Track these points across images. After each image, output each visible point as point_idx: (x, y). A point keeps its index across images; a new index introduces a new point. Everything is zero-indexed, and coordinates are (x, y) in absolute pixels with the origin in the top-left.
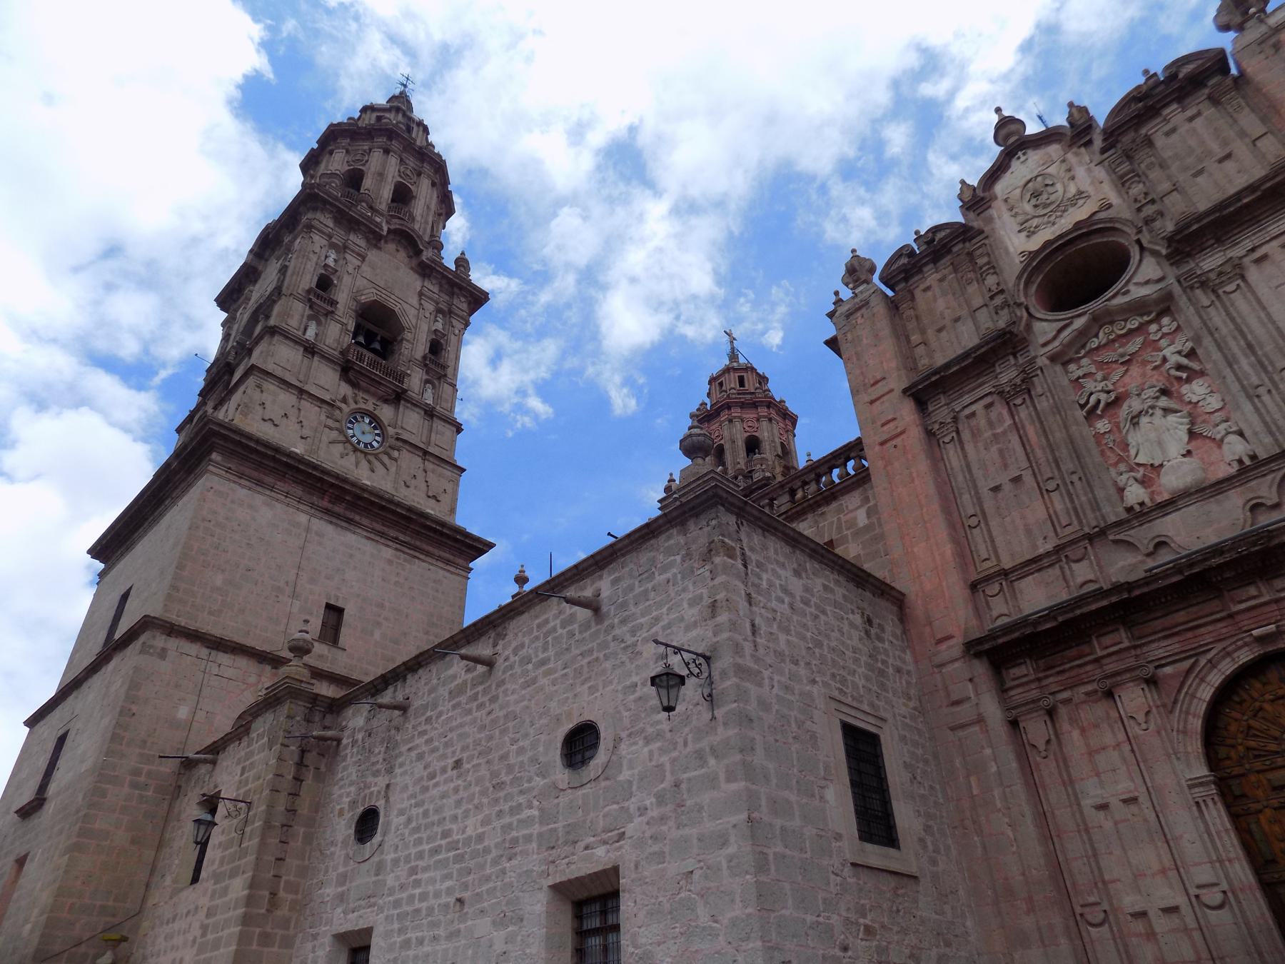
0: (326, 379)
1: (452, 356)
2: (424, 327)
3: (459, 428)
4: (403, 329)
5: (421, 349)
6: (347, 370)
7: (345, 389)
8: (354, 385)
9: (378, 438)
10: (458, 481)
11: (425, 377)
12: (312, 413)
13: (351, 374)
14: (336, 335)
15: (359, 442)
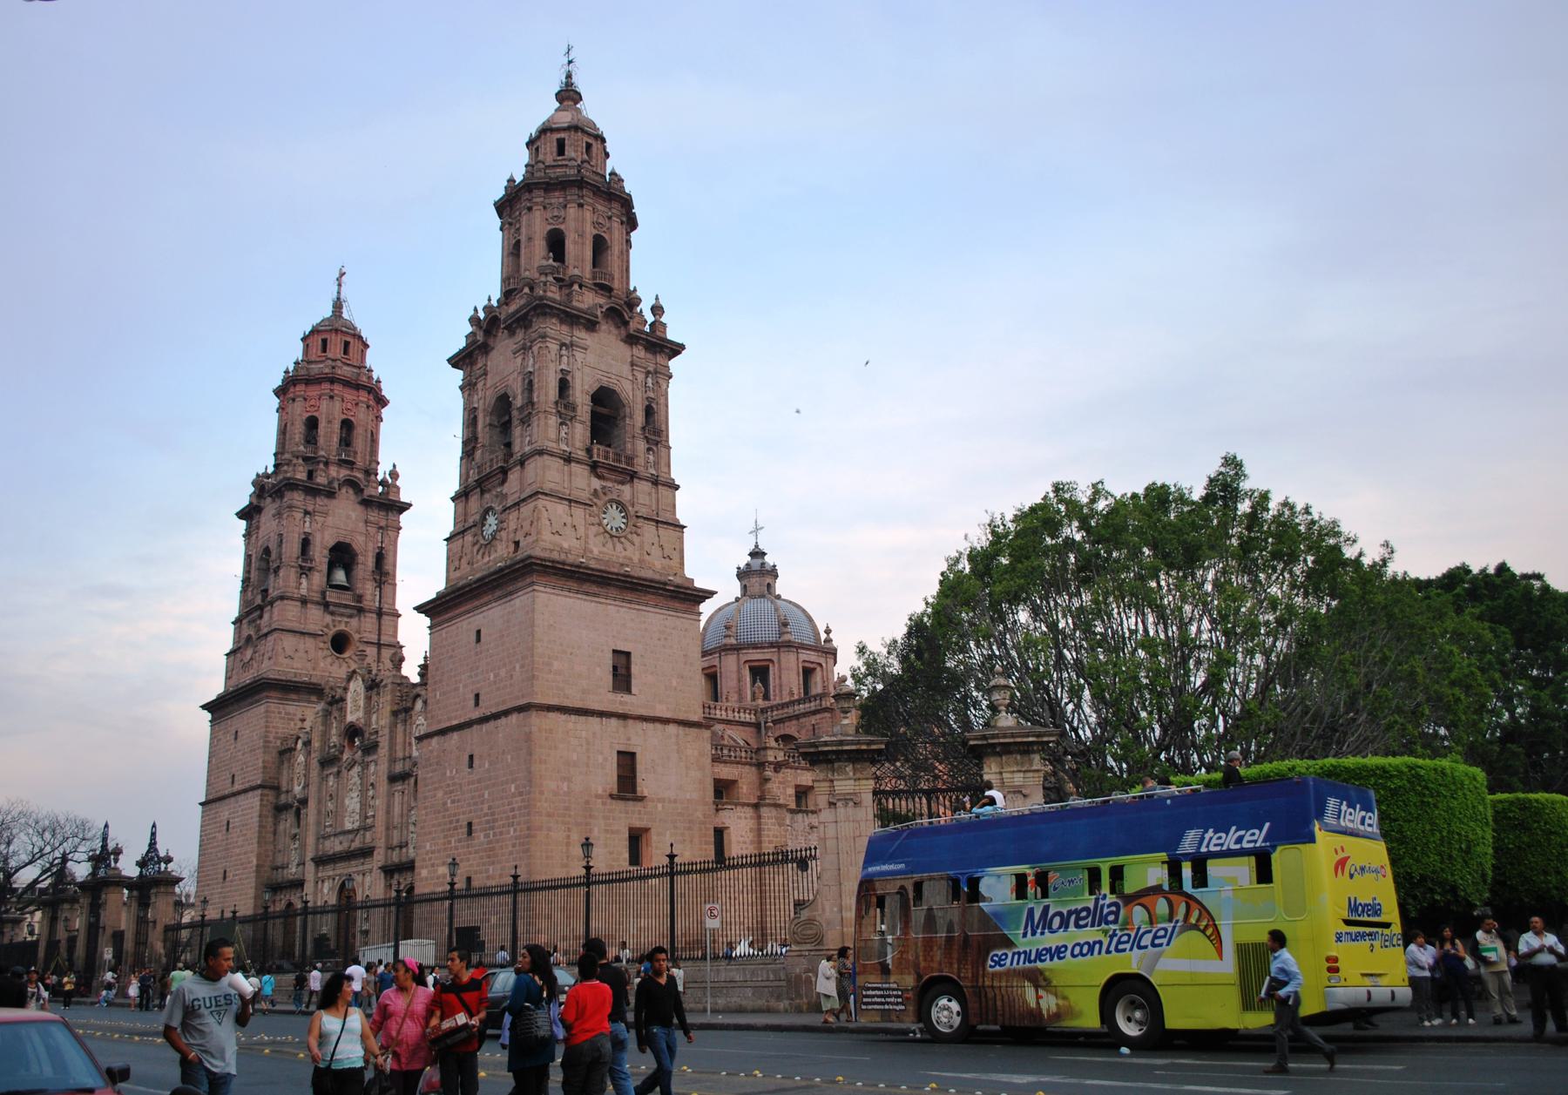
0: (582, 481)
1: (663, 418)
2: (639, 400)
3: (677, 488)
4: (624, 406)
5: (639, 418)
6: (594, 467)
7: (596, 484)
8: (600, 477)
9: (624, 521)
10: (682, 537)
11: (647, 446)
12: (579, 512)
13: (599, 470)
14: (580, 432)
15: (612, 529)
